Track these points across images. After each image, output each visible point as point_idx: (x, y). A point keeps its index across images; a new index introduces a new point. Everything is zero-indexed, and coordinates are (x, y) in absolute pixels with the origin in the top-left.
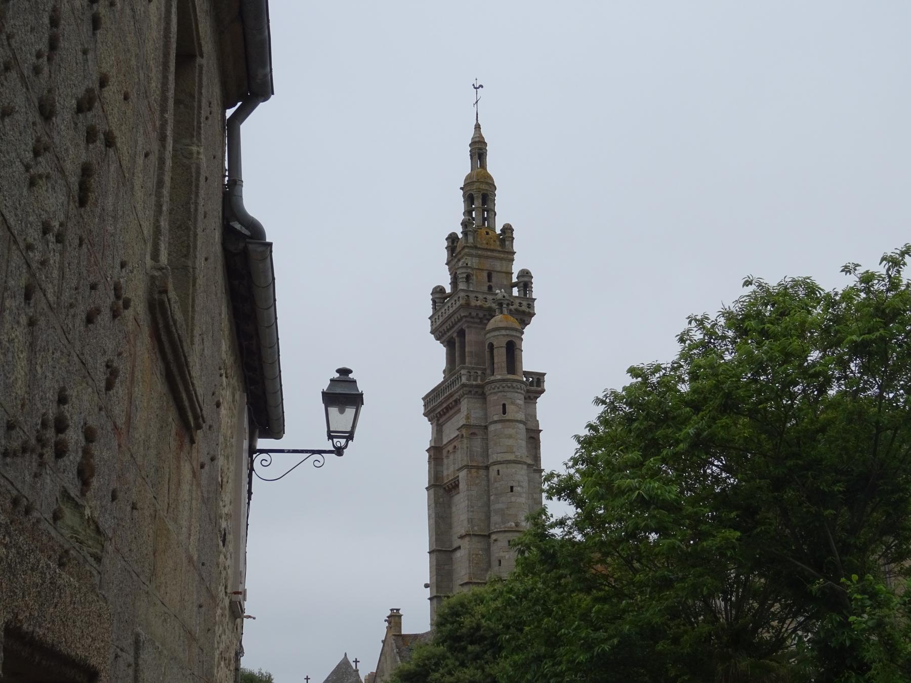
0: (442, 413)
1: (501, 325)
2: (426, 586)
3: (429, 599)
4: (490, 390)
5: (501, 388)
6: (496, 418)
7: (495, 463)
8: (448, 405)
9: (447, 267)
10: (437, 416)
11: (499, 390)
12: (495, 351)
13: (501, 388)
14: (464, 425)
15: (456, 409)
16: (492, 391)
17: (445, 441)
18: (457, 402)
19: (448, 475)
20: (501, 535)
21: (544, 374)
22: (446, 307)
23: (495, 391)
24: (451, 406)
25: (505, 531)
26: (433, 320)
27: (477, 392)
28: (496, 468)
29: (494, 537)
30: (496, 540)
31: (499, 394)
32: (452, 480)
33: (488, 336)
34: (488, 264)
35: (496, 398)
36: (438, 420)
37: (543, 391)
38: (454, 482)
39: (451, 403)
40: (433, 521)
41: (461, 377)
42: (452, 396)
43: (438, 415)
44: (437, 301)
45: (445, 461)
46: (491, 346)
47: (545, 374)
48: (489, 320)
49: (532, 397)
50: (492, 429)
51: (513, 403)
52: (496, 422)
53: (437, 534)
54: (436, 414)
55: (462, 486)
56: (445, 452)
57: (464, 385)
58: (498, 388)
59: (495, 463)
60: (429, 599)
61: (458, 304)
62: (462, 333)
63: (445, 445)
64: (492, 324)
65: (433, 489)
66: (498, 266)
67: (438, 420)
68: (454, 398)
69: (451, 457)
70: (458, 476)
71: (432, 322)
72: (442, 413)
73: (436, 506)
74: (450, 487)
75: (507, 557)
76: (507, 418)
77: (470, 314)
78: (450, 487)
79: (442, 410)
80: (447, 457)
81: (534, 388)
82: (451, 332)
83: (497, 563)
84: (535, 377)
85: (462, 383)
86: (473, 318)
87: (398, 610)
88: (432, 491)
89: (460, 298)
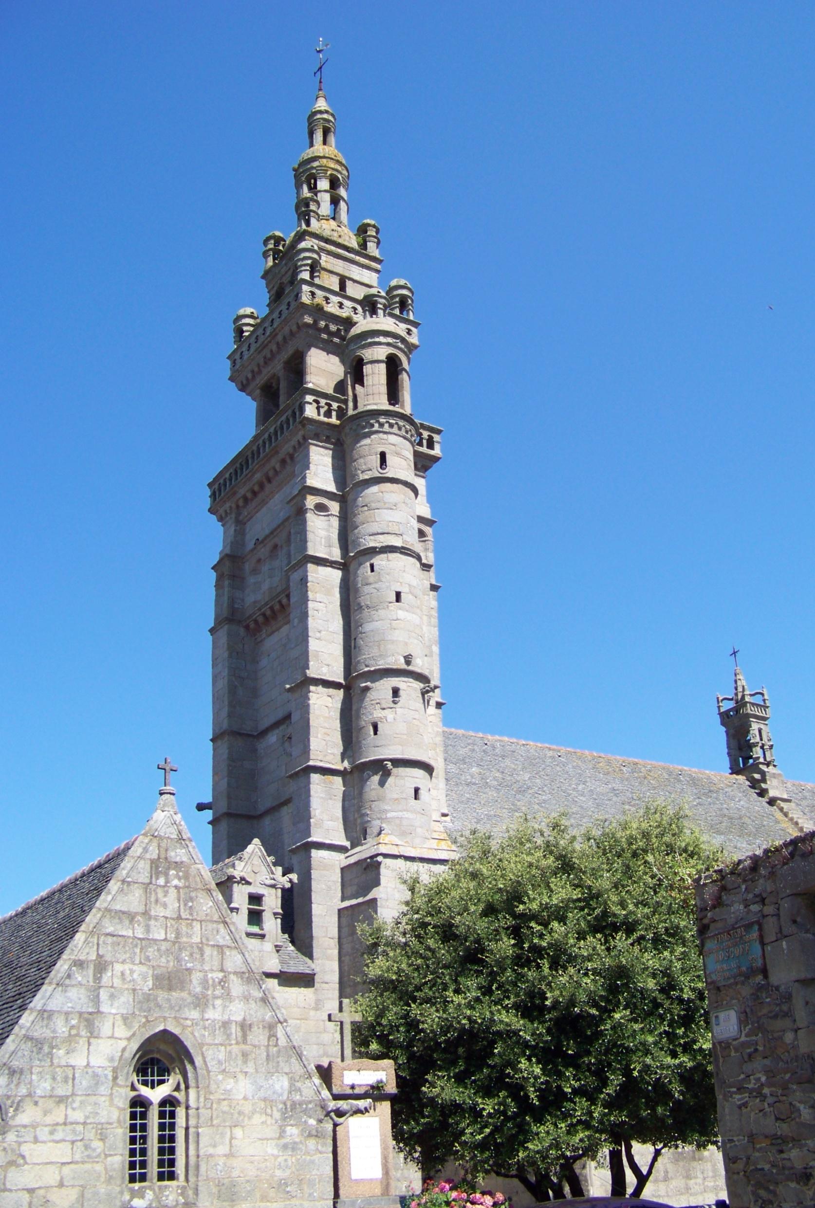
2: (201, 807)
3: (209, 823)
9: (264, 282)
10: (238, 507)
26: (237, 356)
32: (266, 604)
36: (239, 514)
40: (222, 683)
43: (241, 503)
45: (251, 580)
51: (398, 454)
53: (232, 705)
56: (247, 567)
60: (209, 823)
63: (252, 550)
65: (226, 627)
67: (239, 514)
69: (265, 568)
71: (234, 363)
72: (249, 495)
73: (230, 656)
76: (390, 475)
78: (261, 619)
80: (255, 571)
88: (223, 633)
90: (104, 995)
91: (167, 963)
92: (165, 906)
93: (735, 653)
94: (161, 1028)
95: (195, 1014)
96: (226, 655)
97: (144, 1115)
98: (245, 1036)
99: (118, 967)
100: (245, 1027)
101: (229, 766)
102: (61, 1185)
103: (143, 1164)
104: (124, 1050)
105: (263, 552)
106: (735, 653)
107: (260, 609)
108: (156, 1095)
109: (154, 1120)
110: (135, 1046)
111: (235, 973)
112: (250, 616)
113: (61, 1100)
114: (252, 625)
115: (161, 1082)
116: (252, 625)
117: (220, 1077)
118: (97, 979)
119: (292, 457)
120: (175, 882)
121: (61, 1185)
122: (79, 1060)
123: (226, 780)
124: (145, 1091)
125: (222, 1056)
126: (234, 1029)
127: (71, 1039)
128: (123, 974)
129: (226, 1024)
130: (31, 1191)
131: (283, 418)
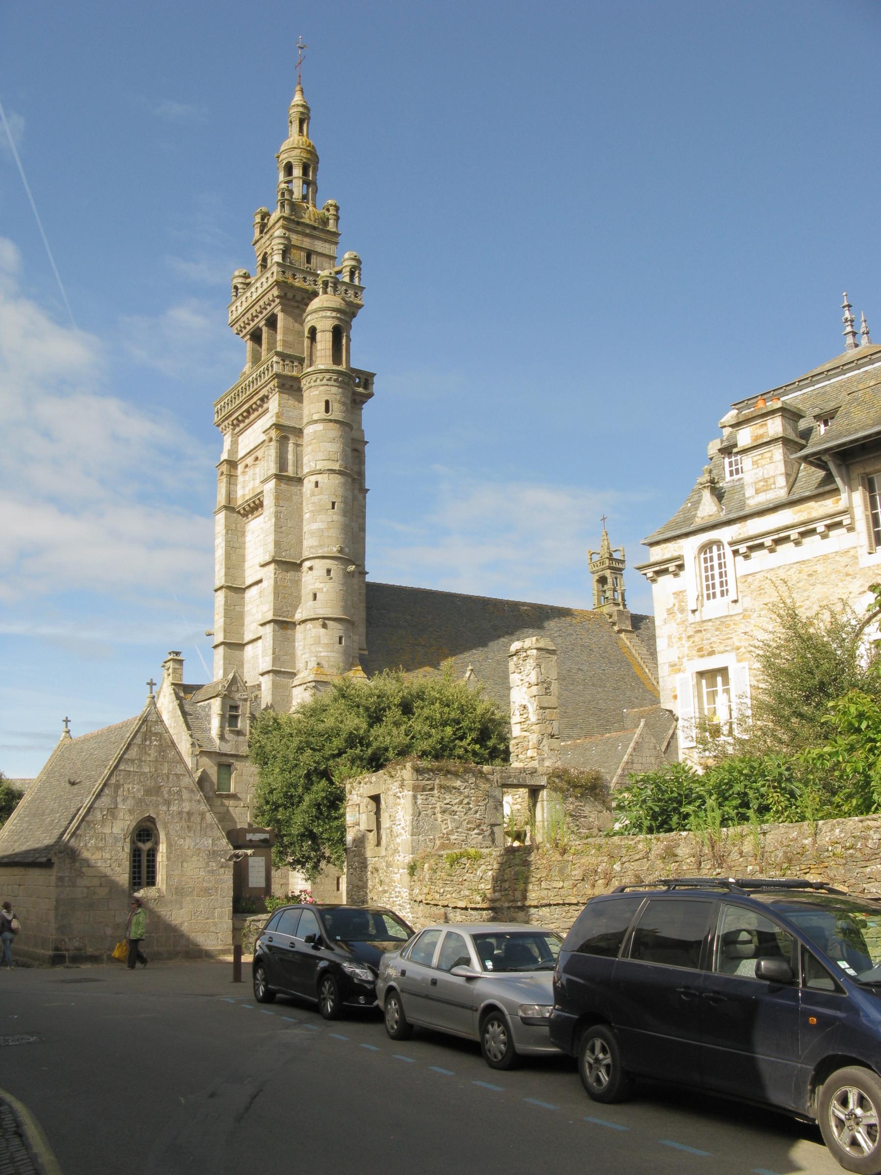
0: (240, 418)
1: (326, 305)
4: (309, 383)
5: (325, 382)
6: (315, 417)
7: (312, 473)
8: (251, 407)
10: (233, 425)
11: (322, 383)
12: (319, 336)
13: (325, 382)
14: (274, 424)
15: (261, 410)
16: (313, 384)
17: (240, 455)
18: (264, 399)
19: (244, 495)
20: (317, 561)
21: (374, 375)
22: (253, 289)
23: (316, 384)
24: (254, 406)
25: (323, 557)
27: (291, 386)
28: (313, 478)
29: (307, 564)
30: (311, 568)
31: (322, 388)
32: (250, 499)
33: (309, 318)
34: (307, 243)
35: (317, 392)
37: (371, 395)
38: (254, 502)
39: (255, 403)
41: (272, 366)
42: (257, 393)
44: (239, 286)
46: (313, 331)
47: (374, 375)
48: (307, 305)
49: (358, 401)
50: (311, 431)
52: (316, 422)
54: (232, 421)
55: (269, 501)
56: (240, 468)
57: (277, 376)
58: (321, 380)
59: (312, 473)
61: (271, 281)
62: (272, 322)
64: (315, 304)
66: (320, 246)
68: (260, 395)
70: (262, 492)
73: (227, 533)
74: (247, 509)
75: (325, 590)
77: (286, 294)
78: (247, 509)
79: (241, 414)
81: (361, 390)
82: (256, 320)
83: (311, 597)
84: (363, 377)
85: (274, 372)
86: (289, 299)
87: (177, 653)
89: (275, 274)
90: (119, 799)
91: (150, 783)
92: (149, 755)
93: (604, 519)
94: (147, 815)
95: (165, 808)
96: (224, 532)
97: (139, 855)
98: (189, 819)
99: (126, 786)
100: (189, 814)
101: (225, 609)
102: (101, 885)
103: (140, 878)
104: (129, 825)
105: (250, 460)
106: (604, 519)
107: (247, 501)
108: (146, 847)
109: (144, 859)
110: (134, 824)
111: (185, 788)
112: (240, 506)
113: (101, 849)
114: (242, 512)
115: (148, 840)
116: (242, 512)
117: (176, 838)
118: (116, 792)
119: (267, 397)
120: (155, 743)
121: (101, 885)
122: (107, 830)
123: (223, 619)
124: (140, 845)
125: (178, 828)
126: (184, 815)
127: (103, 820)
128: (128, 789)
129: (180, 813)
130: (88, 888)
131: (262, 369)
